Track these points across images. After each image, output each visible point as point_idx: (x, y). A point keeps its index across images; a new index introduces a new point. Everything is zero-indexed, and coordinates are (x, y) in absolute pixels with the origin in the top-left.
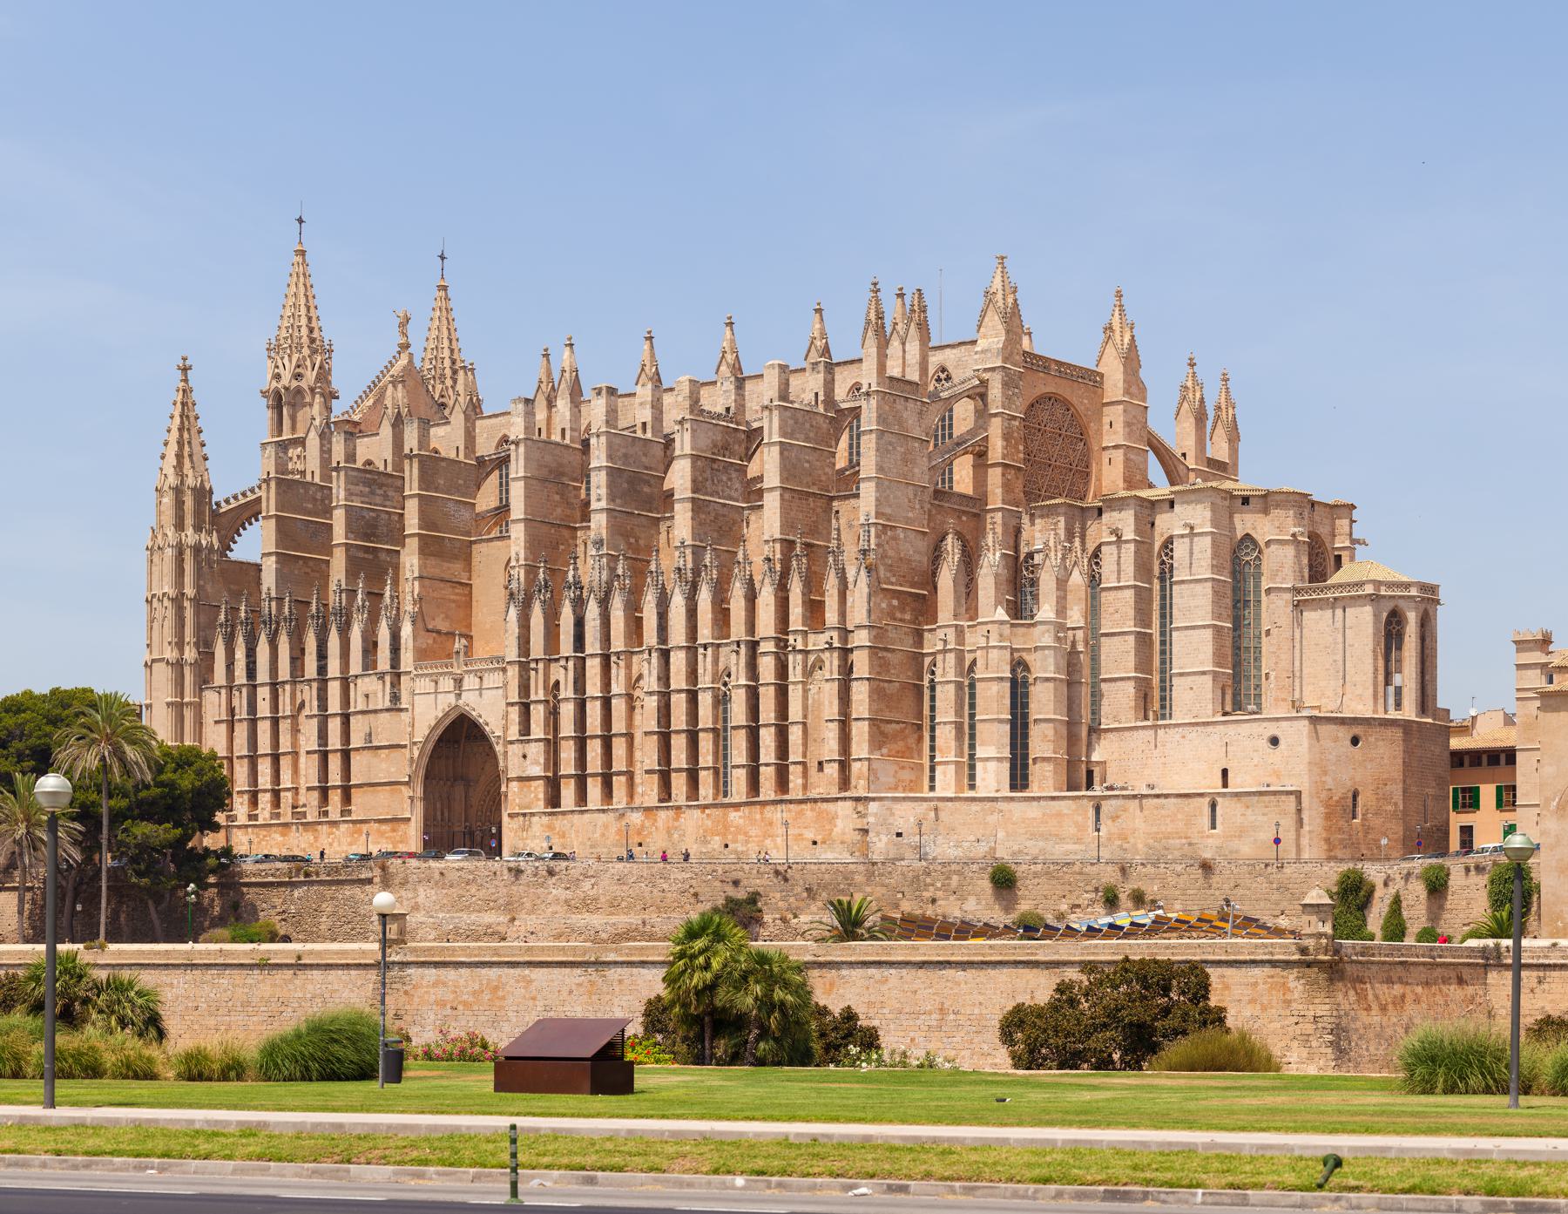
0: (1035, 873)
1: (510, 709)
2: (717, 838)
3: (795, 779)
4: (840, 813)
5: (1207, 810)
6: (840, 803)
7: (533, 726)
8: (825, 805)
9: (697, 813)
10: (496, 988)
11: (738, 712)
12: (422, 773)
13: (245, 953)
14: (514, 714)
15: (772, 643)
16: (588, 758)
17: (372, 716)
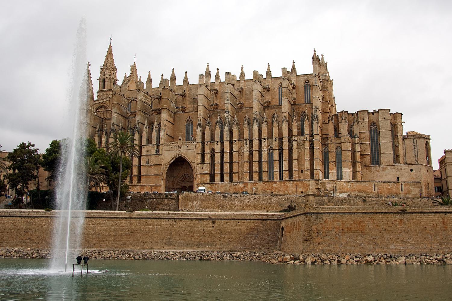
0: (373, 200)
1: (198, 155)
2: (269, 191)
3: (295, 175)
4: (310, 184)
5: (400, 187)
6: (310, 181)
7: (205, 160)
8: (305, 182)
9: (262, 183)
10: (361, 222)
11: (276, 157)
12: (166, 172)
13: (189, 214)
14: (199, 157)
15: (287, 138)
16: (224, 169)
17: (149, 157)
